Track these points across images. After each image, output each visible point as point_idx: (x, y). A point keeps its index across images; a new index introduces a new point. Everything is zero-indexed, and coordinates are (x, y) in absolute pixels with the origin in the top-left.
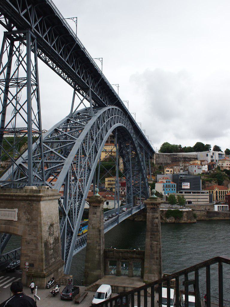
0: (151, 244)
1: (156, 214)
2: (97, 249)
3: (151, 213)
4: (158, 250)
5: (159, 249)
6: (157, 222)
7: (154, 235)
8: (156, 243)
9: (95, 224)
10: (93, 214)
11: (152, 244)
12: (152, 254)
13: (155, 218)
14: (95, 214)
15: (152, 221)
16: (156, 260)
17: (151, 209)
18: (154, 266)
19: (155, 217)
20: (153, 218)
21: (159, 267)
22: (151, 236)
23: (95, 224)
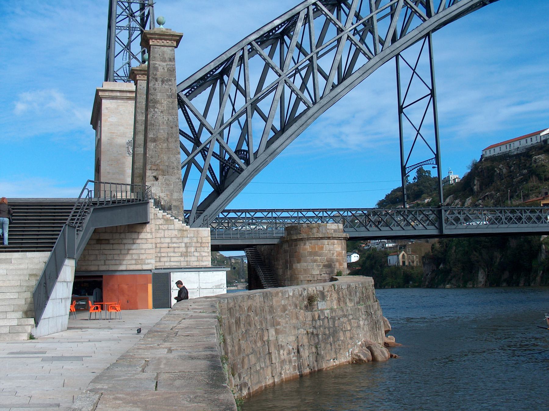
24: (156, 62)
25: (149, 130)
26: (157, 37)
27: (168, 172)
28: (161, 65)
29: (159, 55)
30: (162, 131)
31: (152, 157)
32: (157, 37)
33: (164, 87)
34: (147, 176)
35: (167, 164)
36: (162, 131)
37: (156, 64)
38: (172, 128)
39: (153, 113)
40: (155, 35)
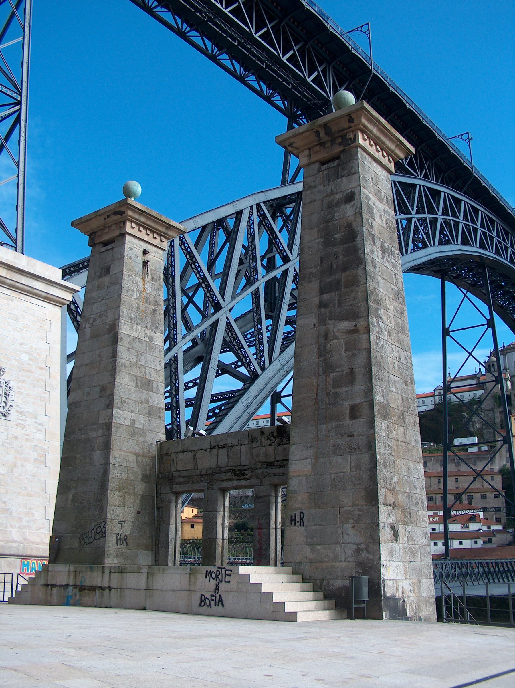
0: (322, 340)
1: (345, 179)
2: (100, 422)
3: (321, 188)
4: (361, 359)
5: (364, 354)
6: (351, 219)
7: (336, 286)
8: (346, 325)
9: (100, 316)
10: (100, 276)
11: (326, 336)
12: (328, 394)
13: (338, 203)
14: (105, 275)
15: (327, 222)
16: (348, 422)
17: (319, 171)
18: (337, 459)
19: (338, 197)
20: (332, 206)
21: (366, 458)
22: (325, 297)
23: (100, 316)
24: (370, 195)
25: (375, 380)
26: (375, 131)
27: (410, 514)
28: (376, 204)
29: (372, 178)
30: (394, 390)
31: (385, 466)
32: (375, 131)
33: (387, 267)
34: (381, 525)
35: (408, 490)
36: (394, 390)
37: (370, 199)
38: (406, 385)
39: (377, 329)
40: (374, 125)
